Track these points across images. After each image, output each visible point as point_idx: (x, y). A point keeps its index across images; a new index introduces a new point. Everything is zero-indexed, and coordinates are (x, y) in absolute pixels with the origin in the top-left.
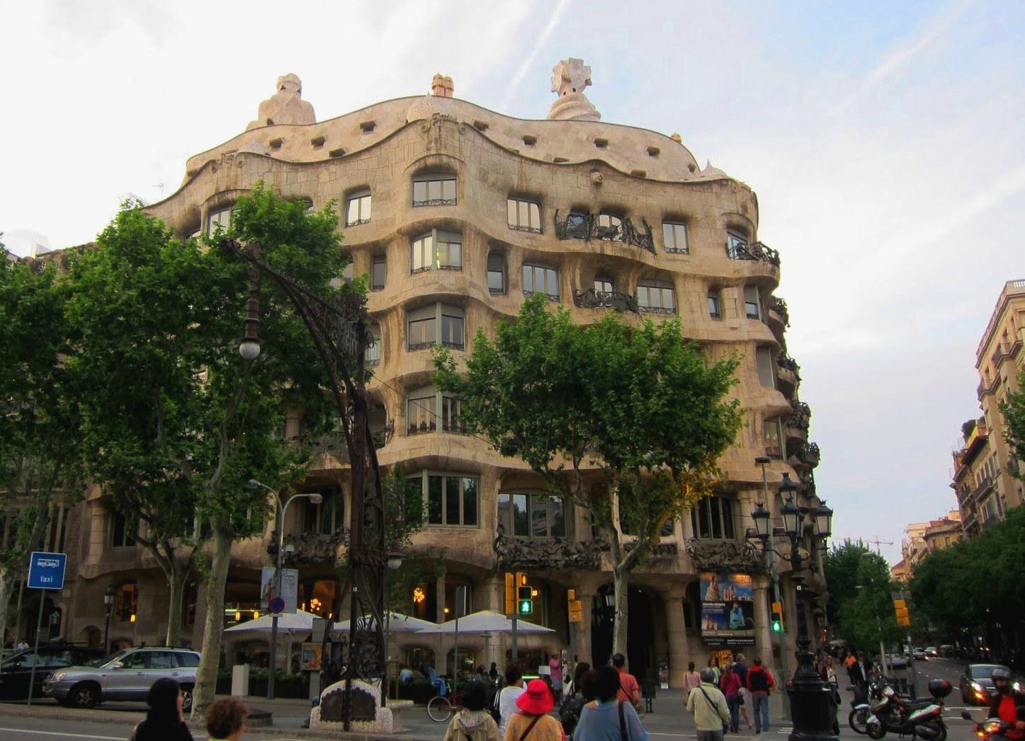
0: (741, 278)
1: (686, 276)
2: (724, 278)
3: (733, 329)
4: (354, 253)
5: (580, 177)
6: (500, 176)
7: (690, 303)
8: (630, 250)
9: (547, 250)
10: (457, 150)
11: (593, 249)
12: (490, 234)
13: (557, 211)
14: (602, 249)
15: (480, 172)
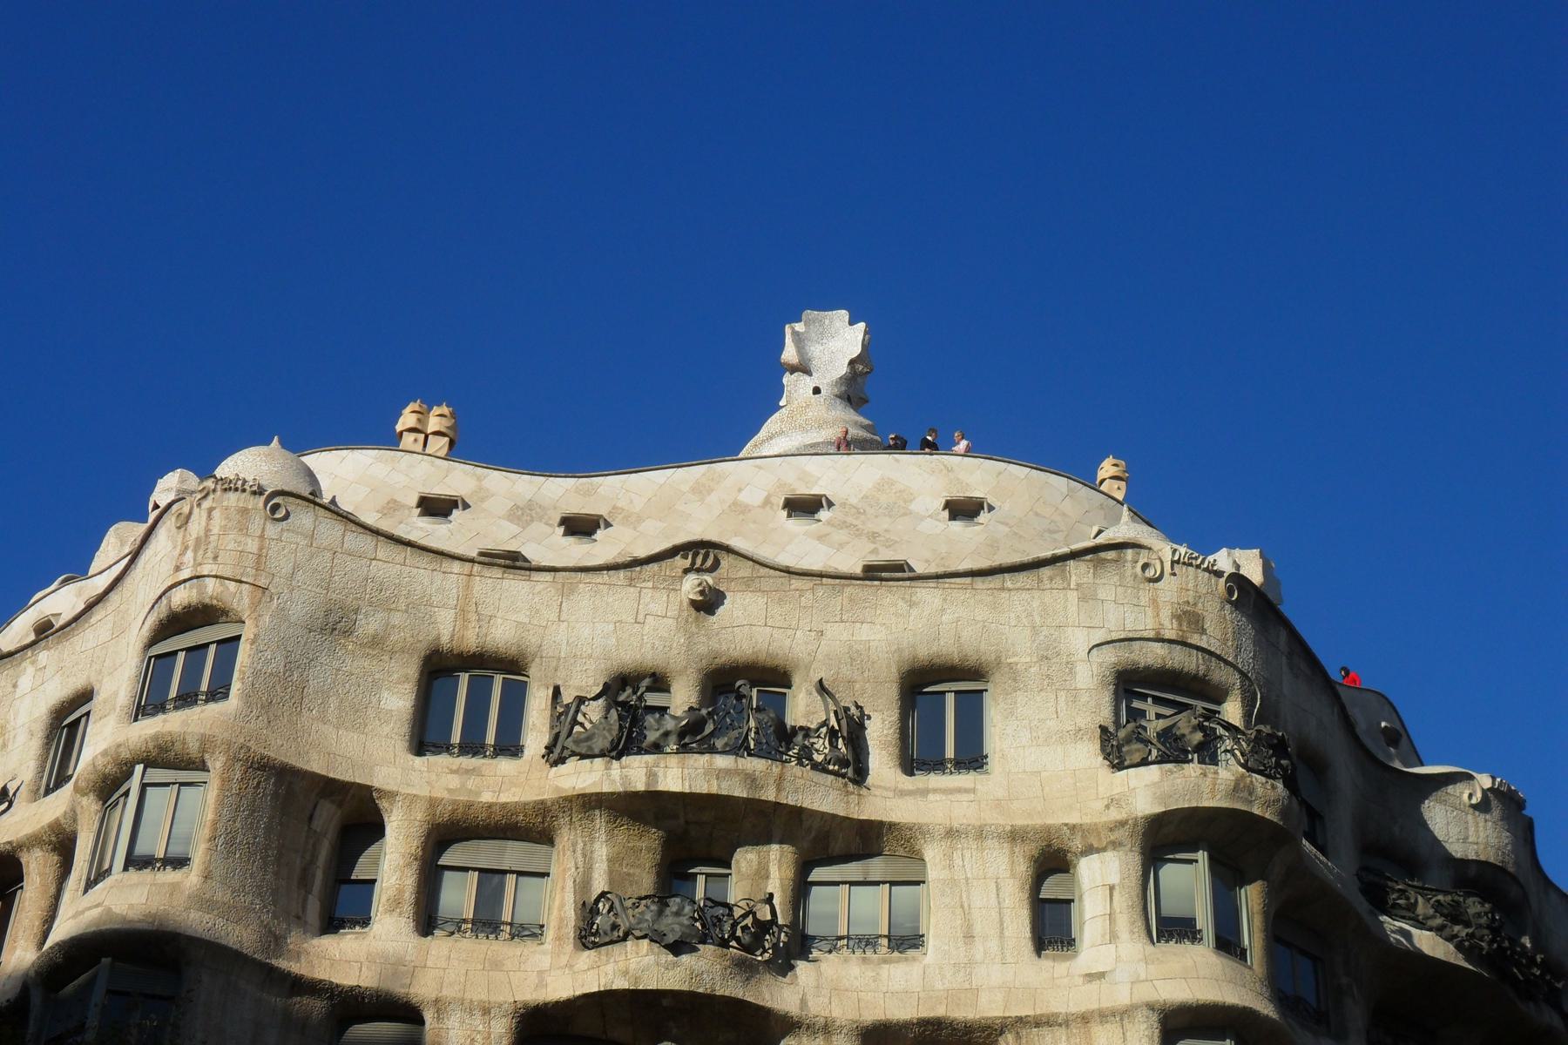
0: (1123, 824)
1: (951, 834)
2: (1073, 828)
3: (1091, 977)
4: (24, 858)
5: (647, 595)
6: (397, 619)
7: (966, 911)
8: (736, 772)
9: (503, 799)
10: (250, 561)
11: (624, 778)
12: (316, 766)
13: (557, 692)
14: (651, 775)
15: (328, 612)
